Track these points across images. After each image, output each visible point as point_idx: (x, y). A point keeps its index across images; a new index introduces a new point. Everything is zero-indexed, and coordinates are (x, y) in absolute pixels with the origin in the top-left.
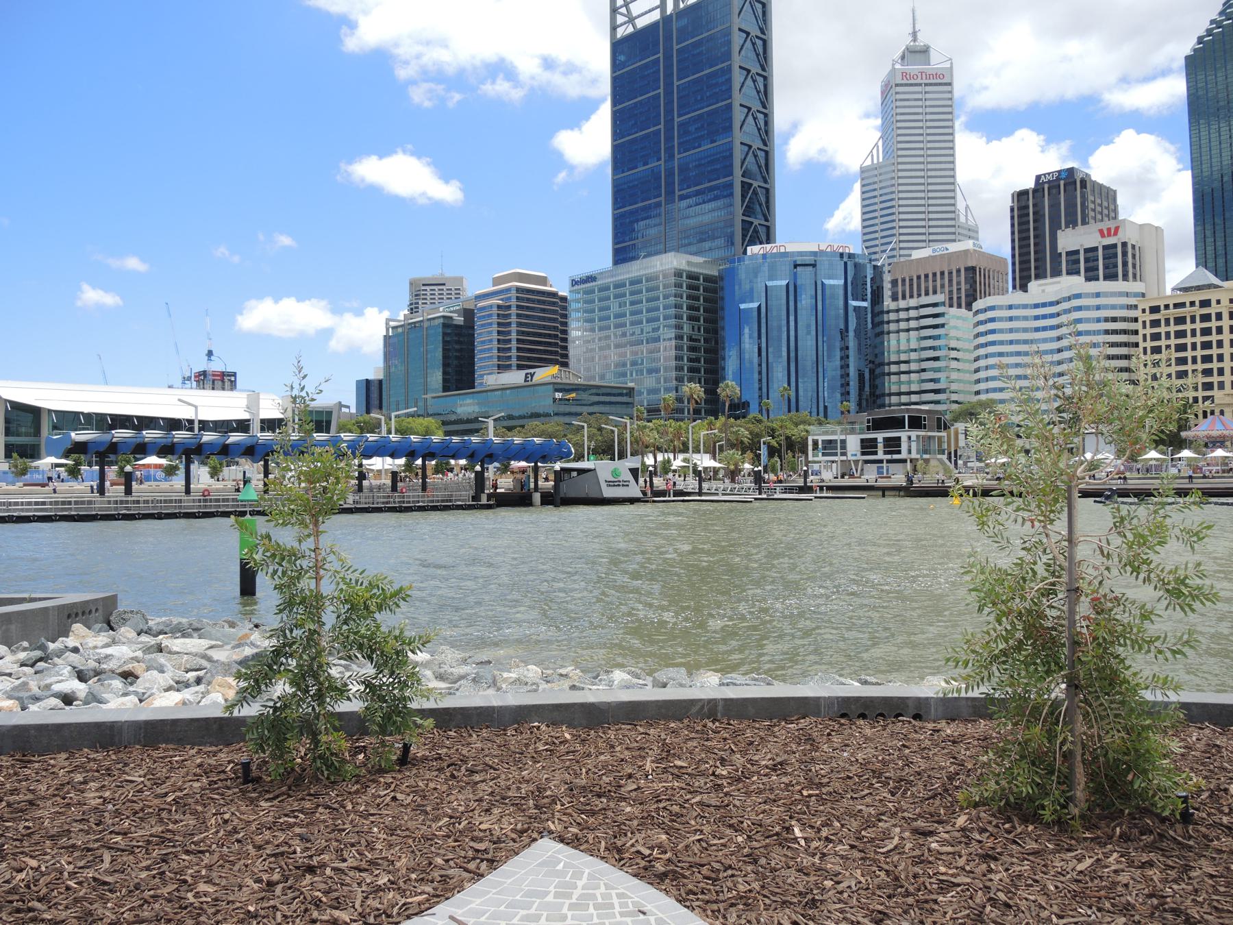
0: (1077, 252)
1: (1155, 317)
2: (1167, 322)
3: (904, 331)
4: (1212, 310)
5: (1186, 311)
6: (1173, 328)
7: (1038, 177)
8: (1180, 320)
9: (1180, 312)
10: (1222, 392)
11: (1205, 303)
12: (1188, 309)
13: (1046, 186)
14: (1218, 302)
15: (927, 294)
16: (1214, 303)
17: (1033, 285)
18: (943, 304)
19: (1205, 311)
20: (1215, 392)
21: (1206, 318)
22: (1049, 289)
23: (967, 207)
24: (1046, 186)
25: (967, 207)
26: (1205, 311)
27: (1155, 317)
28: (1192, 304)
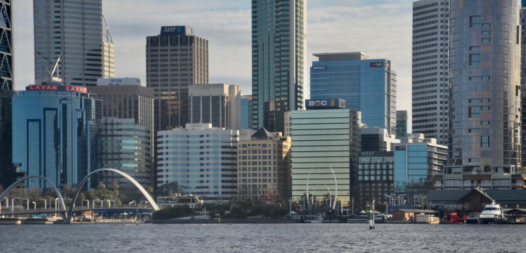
0: (198, 98)
1: (245, 149)
2: (249, 151)
3: (110, 136)
4: (267, 149)
5: (257, 148)
6: (251, 155)
7: (163, 28)
8: (254, 152)
9: (255, 148)
10: (270, 183)
11: (264, 146)
12: (258, 147)
13: (169, 37)
14: (270, 145)
15: (125, 117)
16: (268, 146)
17: (187, 125)
18: (131, 124)
19: (264, 149)
20: (267, 183)
21: (265, 152)
22: (196, 128)
23: (108, 31)
24: (169, 37)
25: (108, 31)
26: (264, 149)
27: (245, 149)
28: (259, 145)
